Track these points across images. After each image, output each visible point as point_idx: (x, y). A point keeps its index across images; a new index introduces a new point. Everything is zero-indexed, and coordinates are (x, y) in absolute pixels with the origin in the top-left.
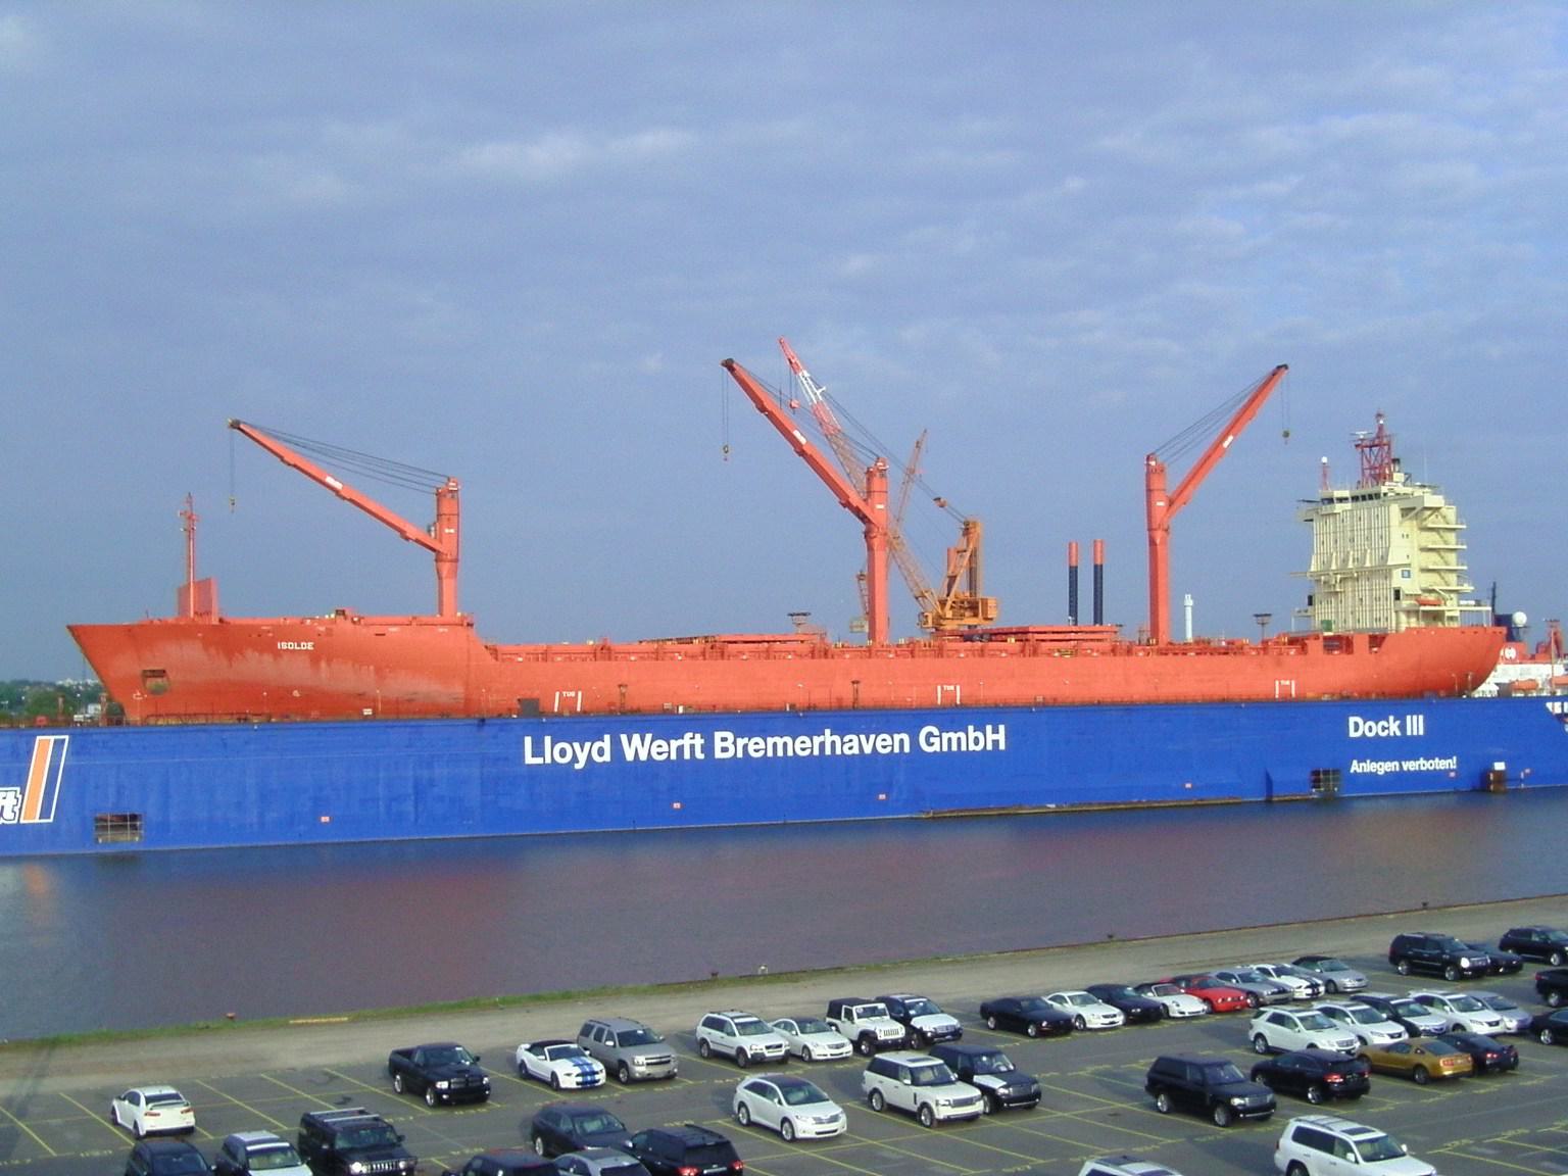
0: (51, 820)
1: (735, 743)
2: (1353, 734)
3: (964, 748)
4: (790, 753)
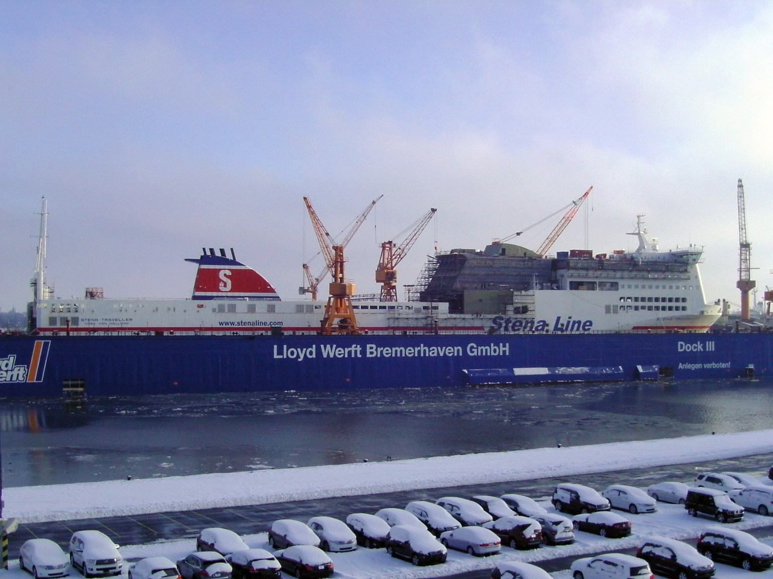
0: (42, 381)
2: (680, 350)
3: (489, 354)
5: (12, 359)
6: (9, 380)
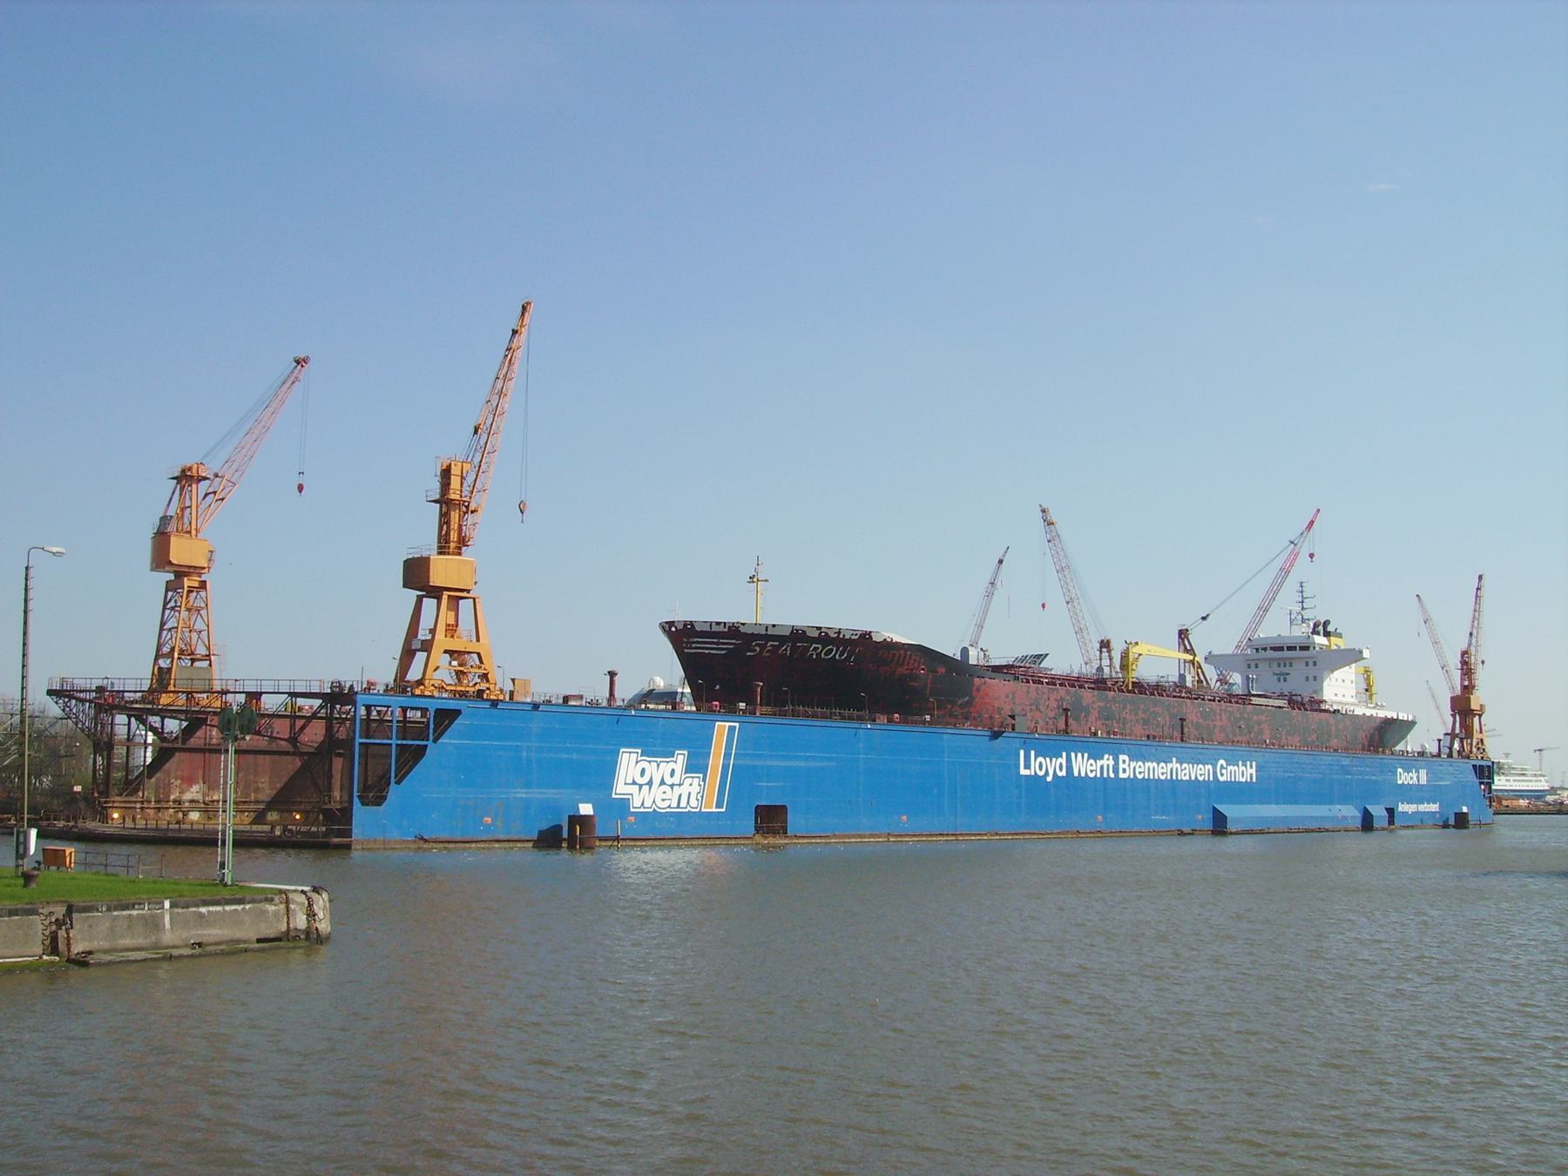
1: (1129, 765)
2: (1400, 782)
4: (1083, 775)
5: (681, 758)
6: (676, 806)
